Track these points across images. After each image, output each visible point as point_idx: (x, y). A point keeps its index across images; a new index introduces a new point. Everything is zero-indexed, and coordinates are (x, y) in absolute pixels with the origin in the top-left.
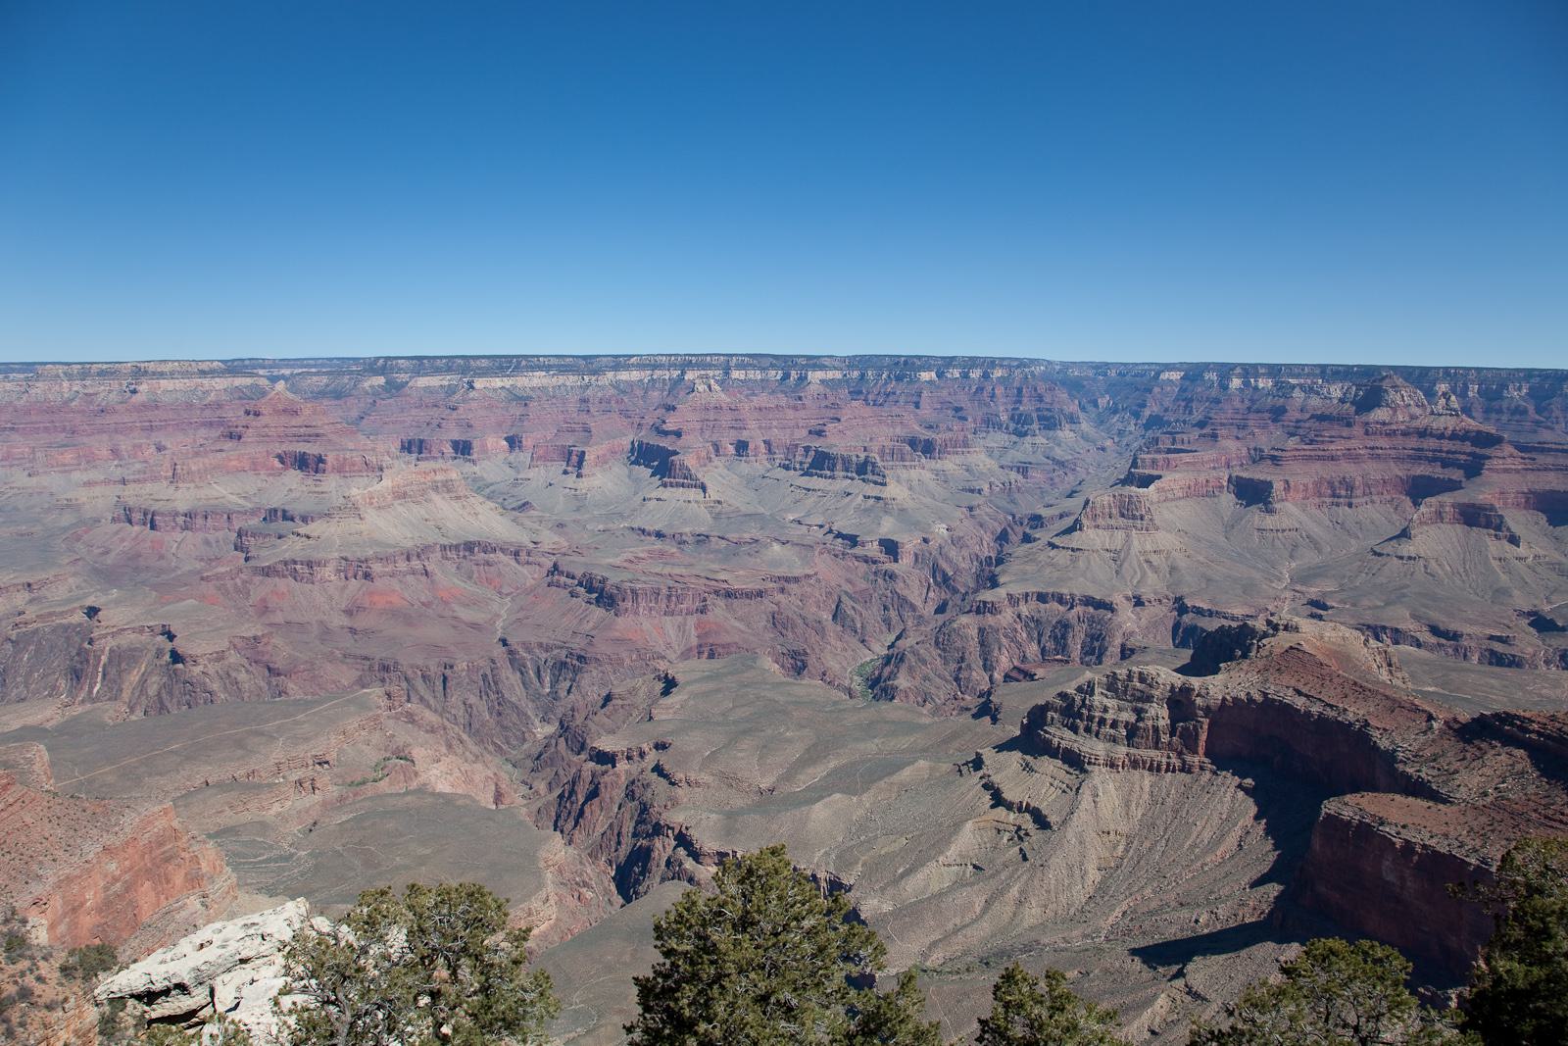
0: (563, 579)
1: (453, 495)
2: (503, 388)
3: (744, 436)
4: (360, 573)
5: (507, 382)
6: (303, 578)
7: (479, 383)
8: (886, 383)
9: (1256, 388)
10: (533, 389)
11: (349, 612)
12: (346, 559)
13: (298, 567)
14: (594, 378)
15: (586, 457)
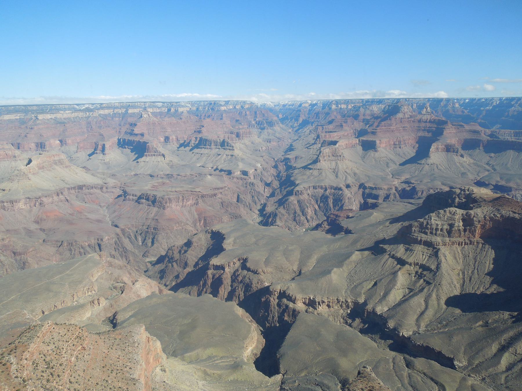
0: (131, 197)
1: (64, 166)
2: (51, 119)
3: (167, 134)
4: (37, 203)
5: (53, 116)
6: (8, 209)
7: (40, 117)
8: (207, 111)
9: (341, 108)
10: (65, 119)
11: (37, 222)
12: (29, 198)
13: (5, 204)
14: (91, 113)
15: (106, 146)
